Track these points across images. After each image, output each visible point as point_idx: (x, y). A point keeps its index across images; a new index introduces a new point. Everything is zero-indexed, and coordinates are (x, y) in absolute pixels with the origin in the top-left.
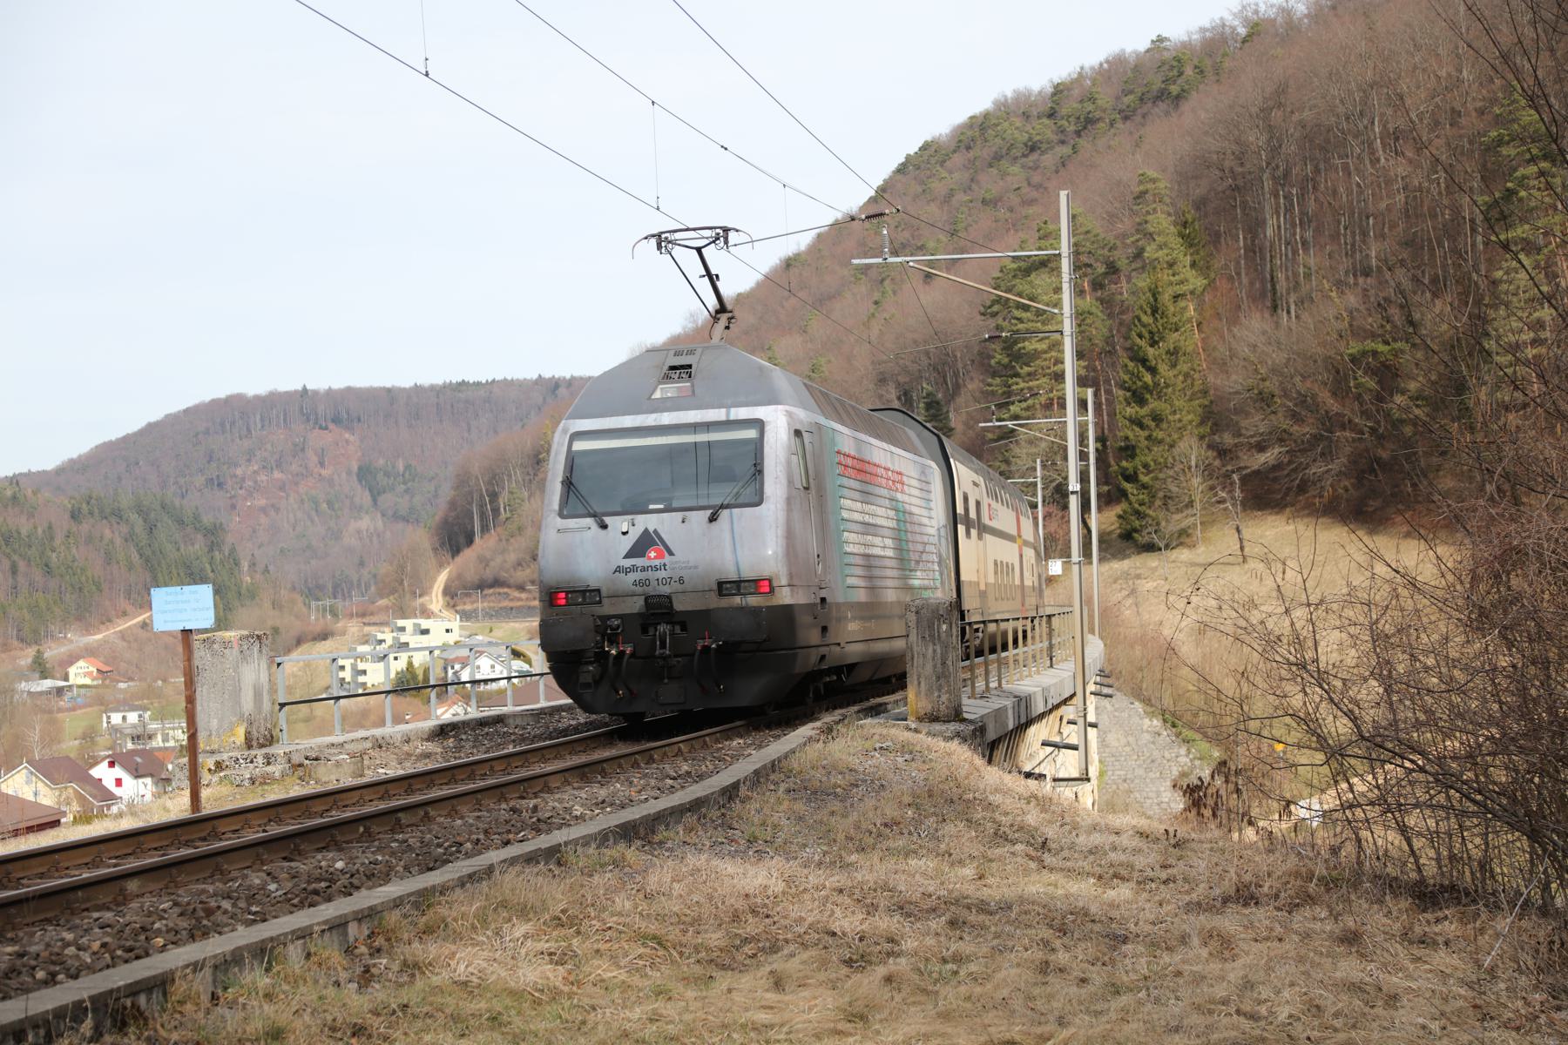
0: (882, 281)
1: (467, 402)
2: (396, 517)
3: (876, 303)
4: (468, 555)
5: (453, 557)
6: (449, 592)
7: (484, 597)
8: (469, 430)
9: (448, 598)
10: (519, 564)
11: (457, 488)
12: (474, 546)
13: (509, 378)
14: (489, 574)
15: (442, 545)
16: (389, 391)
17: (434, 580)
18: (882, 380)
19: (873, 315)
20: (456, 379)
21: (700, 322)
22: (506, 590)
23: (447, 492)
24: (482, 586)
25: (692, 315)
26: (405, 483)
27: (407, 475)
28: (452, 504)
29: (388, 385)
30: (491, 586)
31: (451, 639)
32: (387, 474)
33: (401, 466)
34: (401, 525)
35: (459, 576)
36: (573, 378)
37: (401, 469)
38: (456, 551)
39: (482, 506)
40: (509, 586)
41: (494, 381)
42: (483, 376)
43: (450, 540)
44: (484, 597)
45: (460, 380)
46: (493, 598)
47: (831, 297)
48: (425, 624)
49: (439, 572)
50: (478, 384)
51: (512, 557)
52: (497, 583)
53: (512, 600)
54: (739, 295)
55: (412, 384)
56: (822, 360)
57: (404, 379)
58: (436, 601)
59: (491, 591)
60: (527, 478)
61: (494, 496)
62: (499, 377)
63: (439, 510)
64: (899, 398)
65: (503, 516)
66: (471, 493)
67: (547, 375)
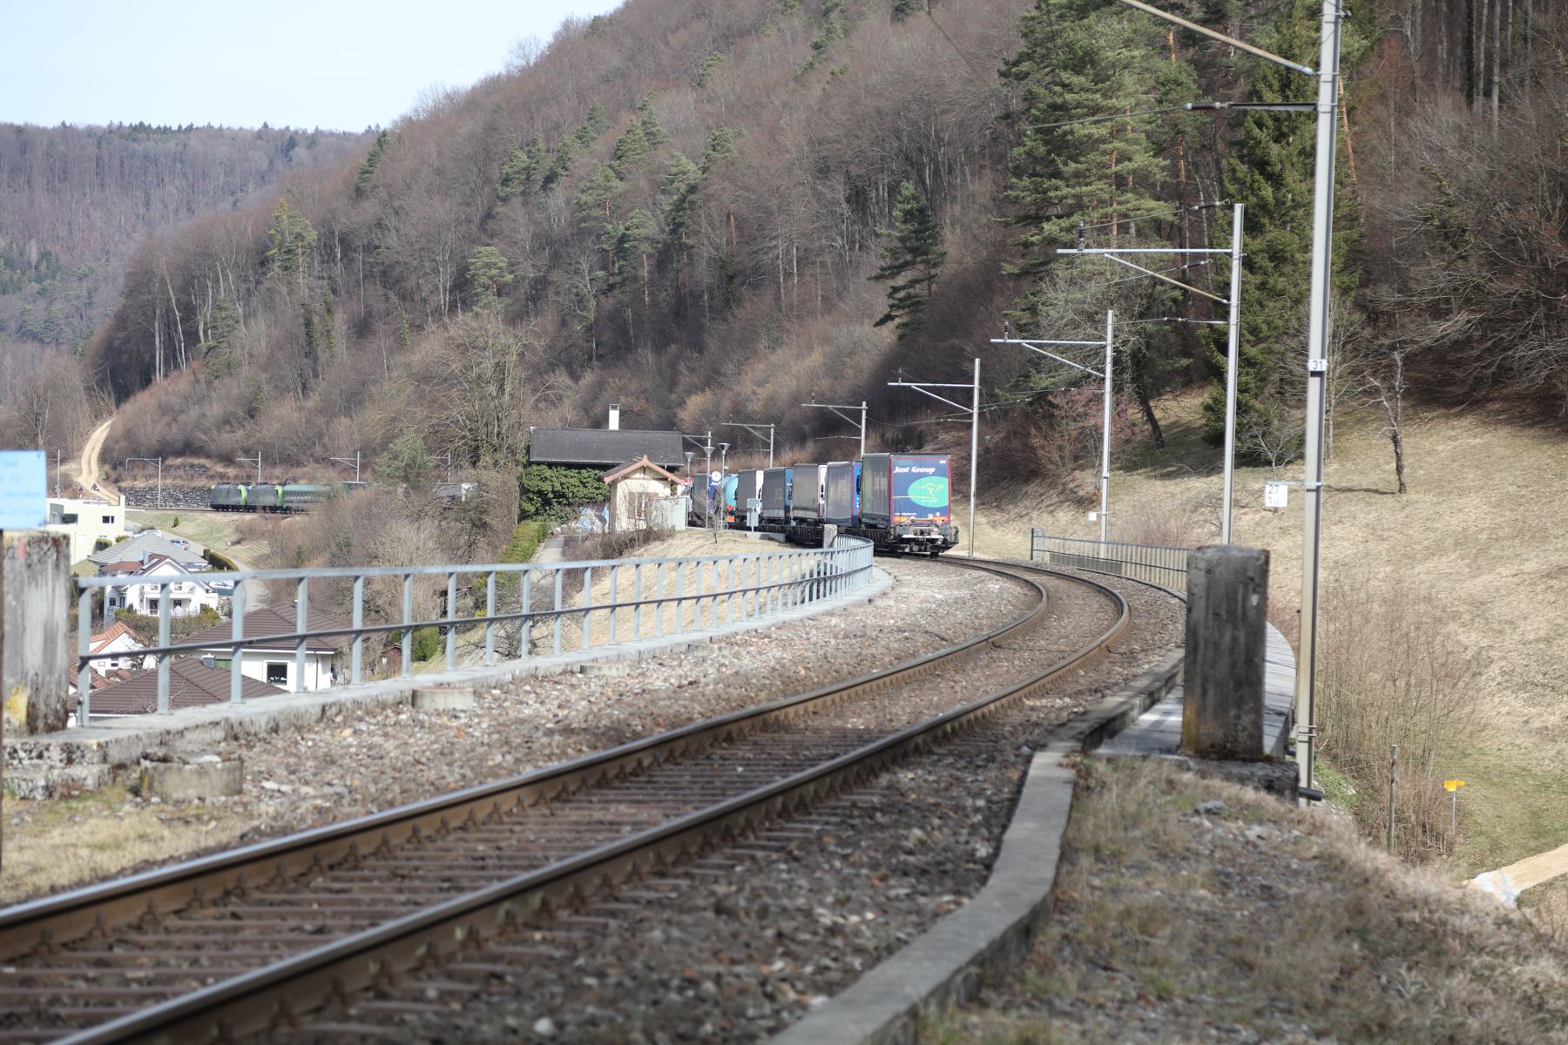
0: (826, 13)
1: (146, 157)
2: (24, 333)
3: (817, 46)
4: (143, 402)
5: (118, 404)
6: (105, 457)
7: (166, 469)
8: (147, 204)
9: (107, 467)
10: (227, 422)
11: (130, 294)
12: (153, 388)
13: (216, 126)
14: (175, 433)
15: (101, 383)
16: (19, 130)
17: (85, 436)
18: (823, 171)
19: (811, 65)
20: (129, 119)
21: (533, 60)
22: (203, 461)
23: (110, 300)
24: (162, 452)
25: (521, 46)
26: (39, 280)
27: (43, 267)
28: (121, 320)
29: (19, 121)
30: (180, 453)
31: (110, 533)
32: (10, 264)
33: (33, 252)
34: (30, 347)
35: (128, 434)
36: (318, 133)
37: (34, 257)
38: (122, 395)
39: (169, 325)
40: (208, 456)
41: (190, 128)
42: (174, 119)
43: (113, 376)
44: (166, 469)
45: (136, 122)
46: (181, 472)
47: (743, 33)
48: (70, 507)
49: (94, 426)
50: (165, 131)
51: (215, 410)
52: (188, 448)
53: (212, 477)
54: (597, 19)
55: (57, 123)
56: (729, 132)
57: (48, 119)
58: (87, 469)
59: (179, 461)
60: (245, 286)
61: (189, 312)
62: (200, 123)
63: (100, 328)
64: (848, 201)
65: (203, 345)
66: (152, 304)
67: (277, 124)
